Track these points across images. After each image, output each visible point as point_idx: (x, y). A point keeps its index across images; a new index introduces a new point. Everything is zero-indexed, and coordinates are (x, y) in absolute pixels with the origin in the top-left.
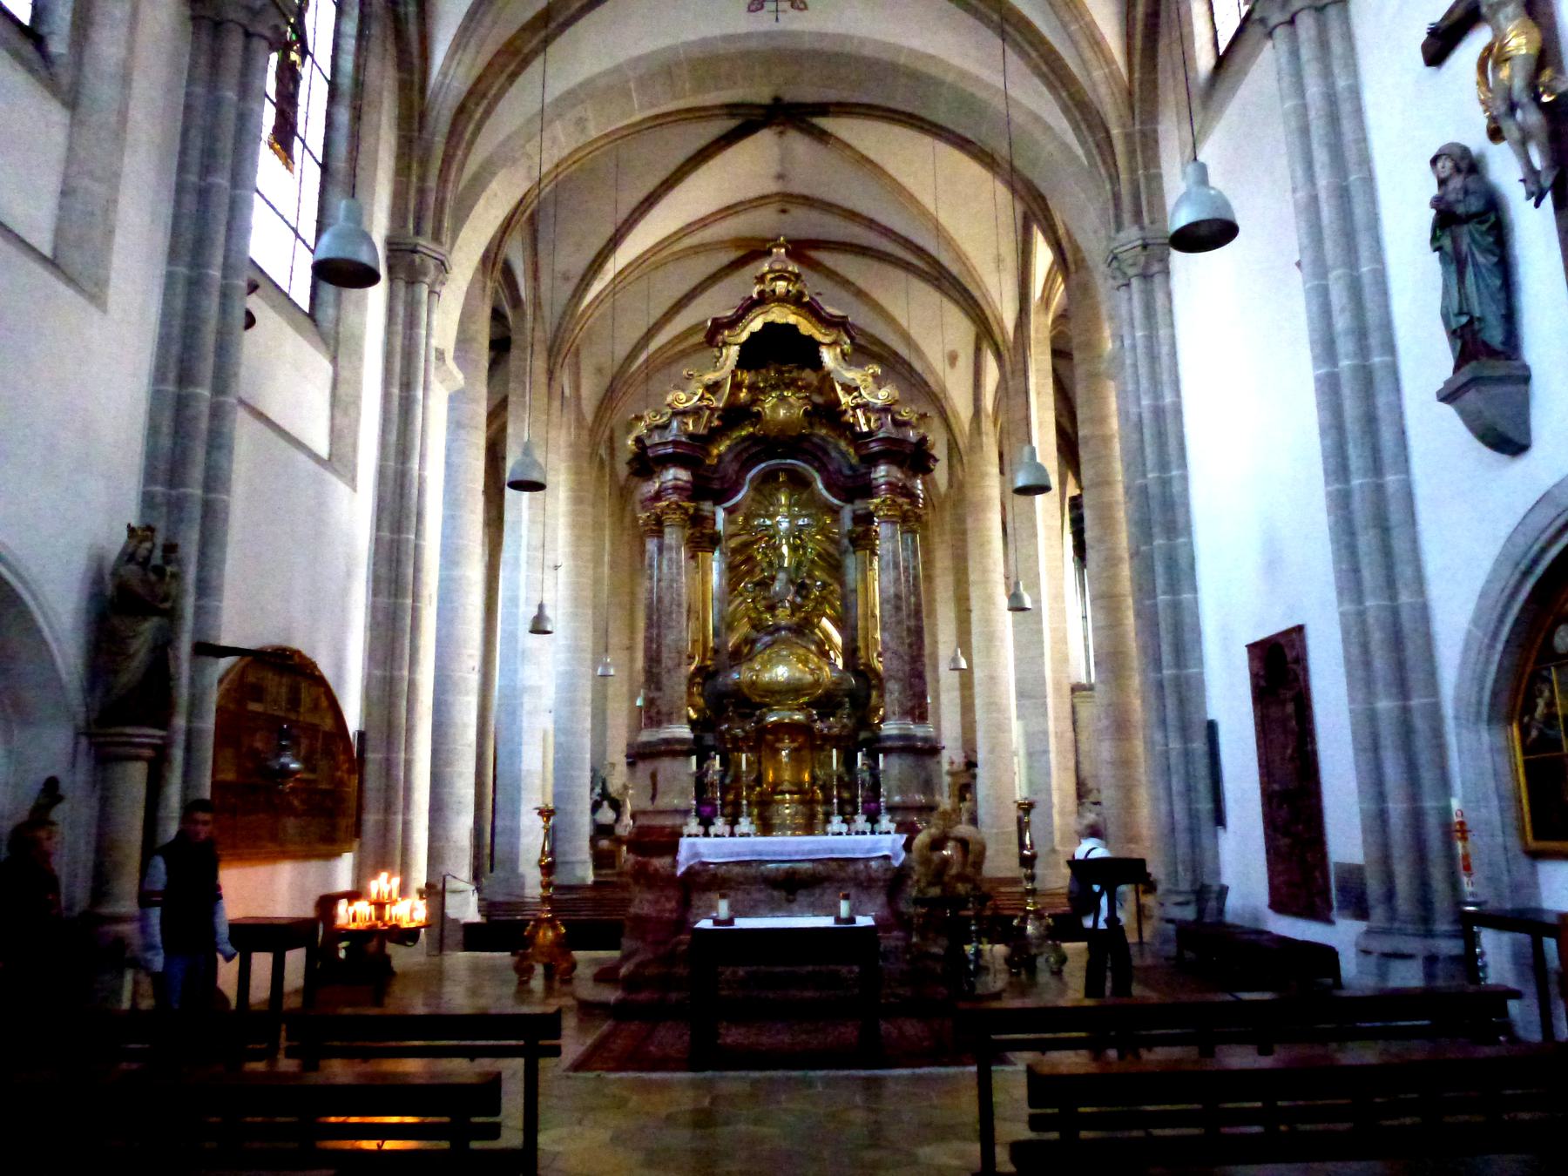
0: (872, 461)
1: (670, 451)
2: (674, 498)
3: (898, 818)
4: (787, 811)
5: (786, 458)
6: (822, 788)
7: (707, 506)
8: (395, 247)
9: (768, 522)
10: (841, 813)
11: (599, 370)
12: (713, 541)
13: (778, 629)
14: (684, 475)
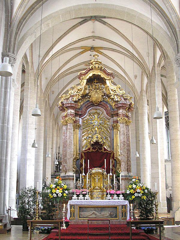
0: (119, 108)
2: (71, 117)
5: (97, 106)
7: (78, 118)
8: (4, 55)
9: (92, 122)
11: (46, 78)
12: (79, 127)
14: (73, 111)
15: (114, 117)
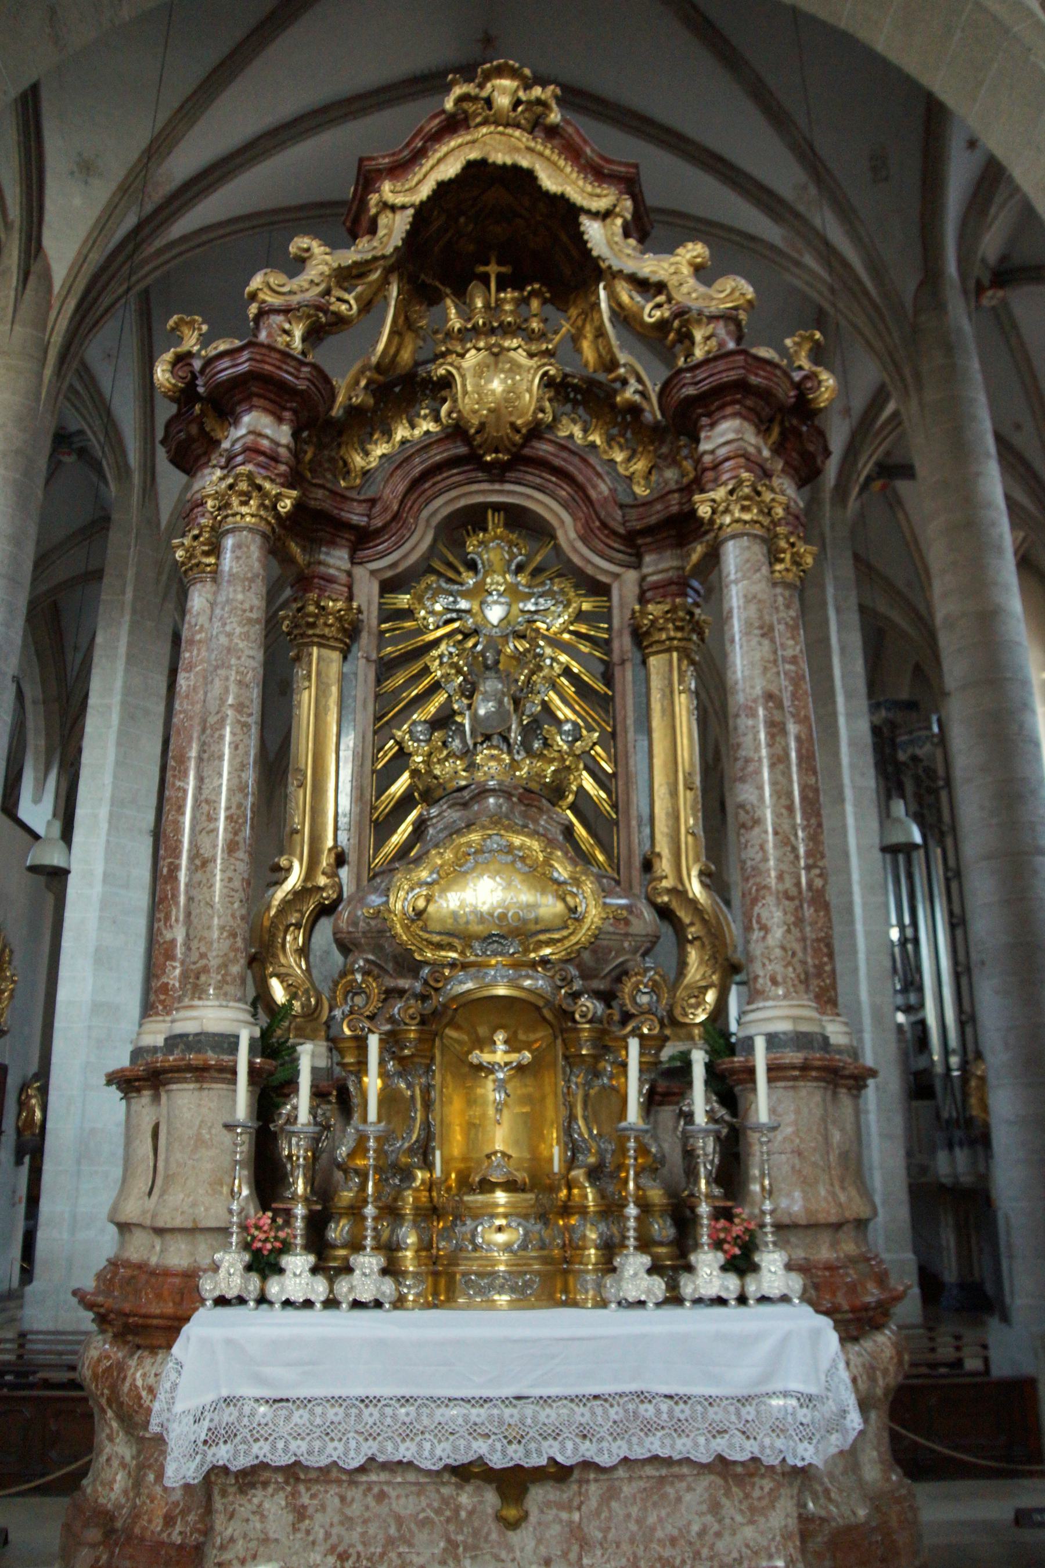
1: (245, 367)
3: (800, 1254)
4: (501, 1238)
5: (502, 481)
6: (595, 1174)
9: (463, 604)
10: (644, 1245)
13: (484, 792)
15: (648, 559)
